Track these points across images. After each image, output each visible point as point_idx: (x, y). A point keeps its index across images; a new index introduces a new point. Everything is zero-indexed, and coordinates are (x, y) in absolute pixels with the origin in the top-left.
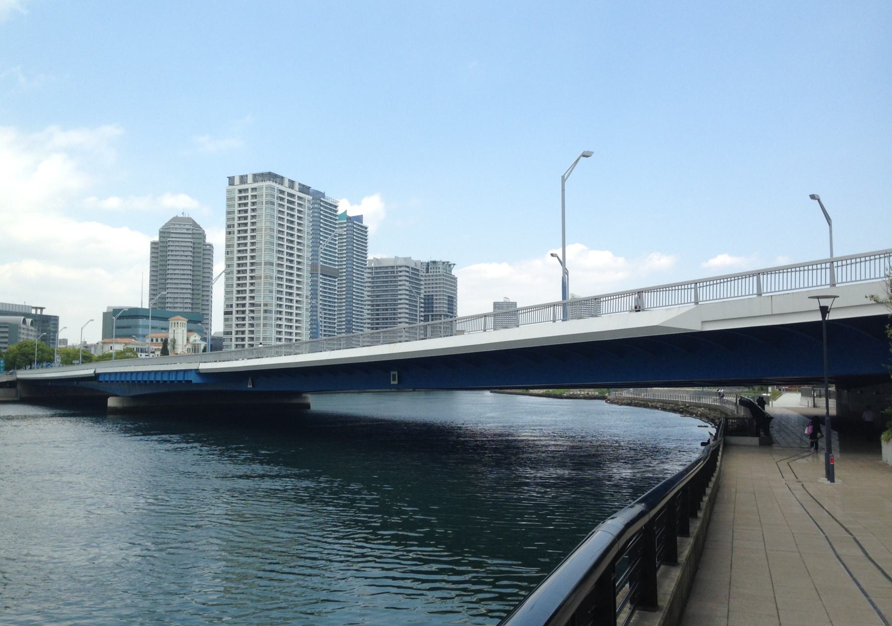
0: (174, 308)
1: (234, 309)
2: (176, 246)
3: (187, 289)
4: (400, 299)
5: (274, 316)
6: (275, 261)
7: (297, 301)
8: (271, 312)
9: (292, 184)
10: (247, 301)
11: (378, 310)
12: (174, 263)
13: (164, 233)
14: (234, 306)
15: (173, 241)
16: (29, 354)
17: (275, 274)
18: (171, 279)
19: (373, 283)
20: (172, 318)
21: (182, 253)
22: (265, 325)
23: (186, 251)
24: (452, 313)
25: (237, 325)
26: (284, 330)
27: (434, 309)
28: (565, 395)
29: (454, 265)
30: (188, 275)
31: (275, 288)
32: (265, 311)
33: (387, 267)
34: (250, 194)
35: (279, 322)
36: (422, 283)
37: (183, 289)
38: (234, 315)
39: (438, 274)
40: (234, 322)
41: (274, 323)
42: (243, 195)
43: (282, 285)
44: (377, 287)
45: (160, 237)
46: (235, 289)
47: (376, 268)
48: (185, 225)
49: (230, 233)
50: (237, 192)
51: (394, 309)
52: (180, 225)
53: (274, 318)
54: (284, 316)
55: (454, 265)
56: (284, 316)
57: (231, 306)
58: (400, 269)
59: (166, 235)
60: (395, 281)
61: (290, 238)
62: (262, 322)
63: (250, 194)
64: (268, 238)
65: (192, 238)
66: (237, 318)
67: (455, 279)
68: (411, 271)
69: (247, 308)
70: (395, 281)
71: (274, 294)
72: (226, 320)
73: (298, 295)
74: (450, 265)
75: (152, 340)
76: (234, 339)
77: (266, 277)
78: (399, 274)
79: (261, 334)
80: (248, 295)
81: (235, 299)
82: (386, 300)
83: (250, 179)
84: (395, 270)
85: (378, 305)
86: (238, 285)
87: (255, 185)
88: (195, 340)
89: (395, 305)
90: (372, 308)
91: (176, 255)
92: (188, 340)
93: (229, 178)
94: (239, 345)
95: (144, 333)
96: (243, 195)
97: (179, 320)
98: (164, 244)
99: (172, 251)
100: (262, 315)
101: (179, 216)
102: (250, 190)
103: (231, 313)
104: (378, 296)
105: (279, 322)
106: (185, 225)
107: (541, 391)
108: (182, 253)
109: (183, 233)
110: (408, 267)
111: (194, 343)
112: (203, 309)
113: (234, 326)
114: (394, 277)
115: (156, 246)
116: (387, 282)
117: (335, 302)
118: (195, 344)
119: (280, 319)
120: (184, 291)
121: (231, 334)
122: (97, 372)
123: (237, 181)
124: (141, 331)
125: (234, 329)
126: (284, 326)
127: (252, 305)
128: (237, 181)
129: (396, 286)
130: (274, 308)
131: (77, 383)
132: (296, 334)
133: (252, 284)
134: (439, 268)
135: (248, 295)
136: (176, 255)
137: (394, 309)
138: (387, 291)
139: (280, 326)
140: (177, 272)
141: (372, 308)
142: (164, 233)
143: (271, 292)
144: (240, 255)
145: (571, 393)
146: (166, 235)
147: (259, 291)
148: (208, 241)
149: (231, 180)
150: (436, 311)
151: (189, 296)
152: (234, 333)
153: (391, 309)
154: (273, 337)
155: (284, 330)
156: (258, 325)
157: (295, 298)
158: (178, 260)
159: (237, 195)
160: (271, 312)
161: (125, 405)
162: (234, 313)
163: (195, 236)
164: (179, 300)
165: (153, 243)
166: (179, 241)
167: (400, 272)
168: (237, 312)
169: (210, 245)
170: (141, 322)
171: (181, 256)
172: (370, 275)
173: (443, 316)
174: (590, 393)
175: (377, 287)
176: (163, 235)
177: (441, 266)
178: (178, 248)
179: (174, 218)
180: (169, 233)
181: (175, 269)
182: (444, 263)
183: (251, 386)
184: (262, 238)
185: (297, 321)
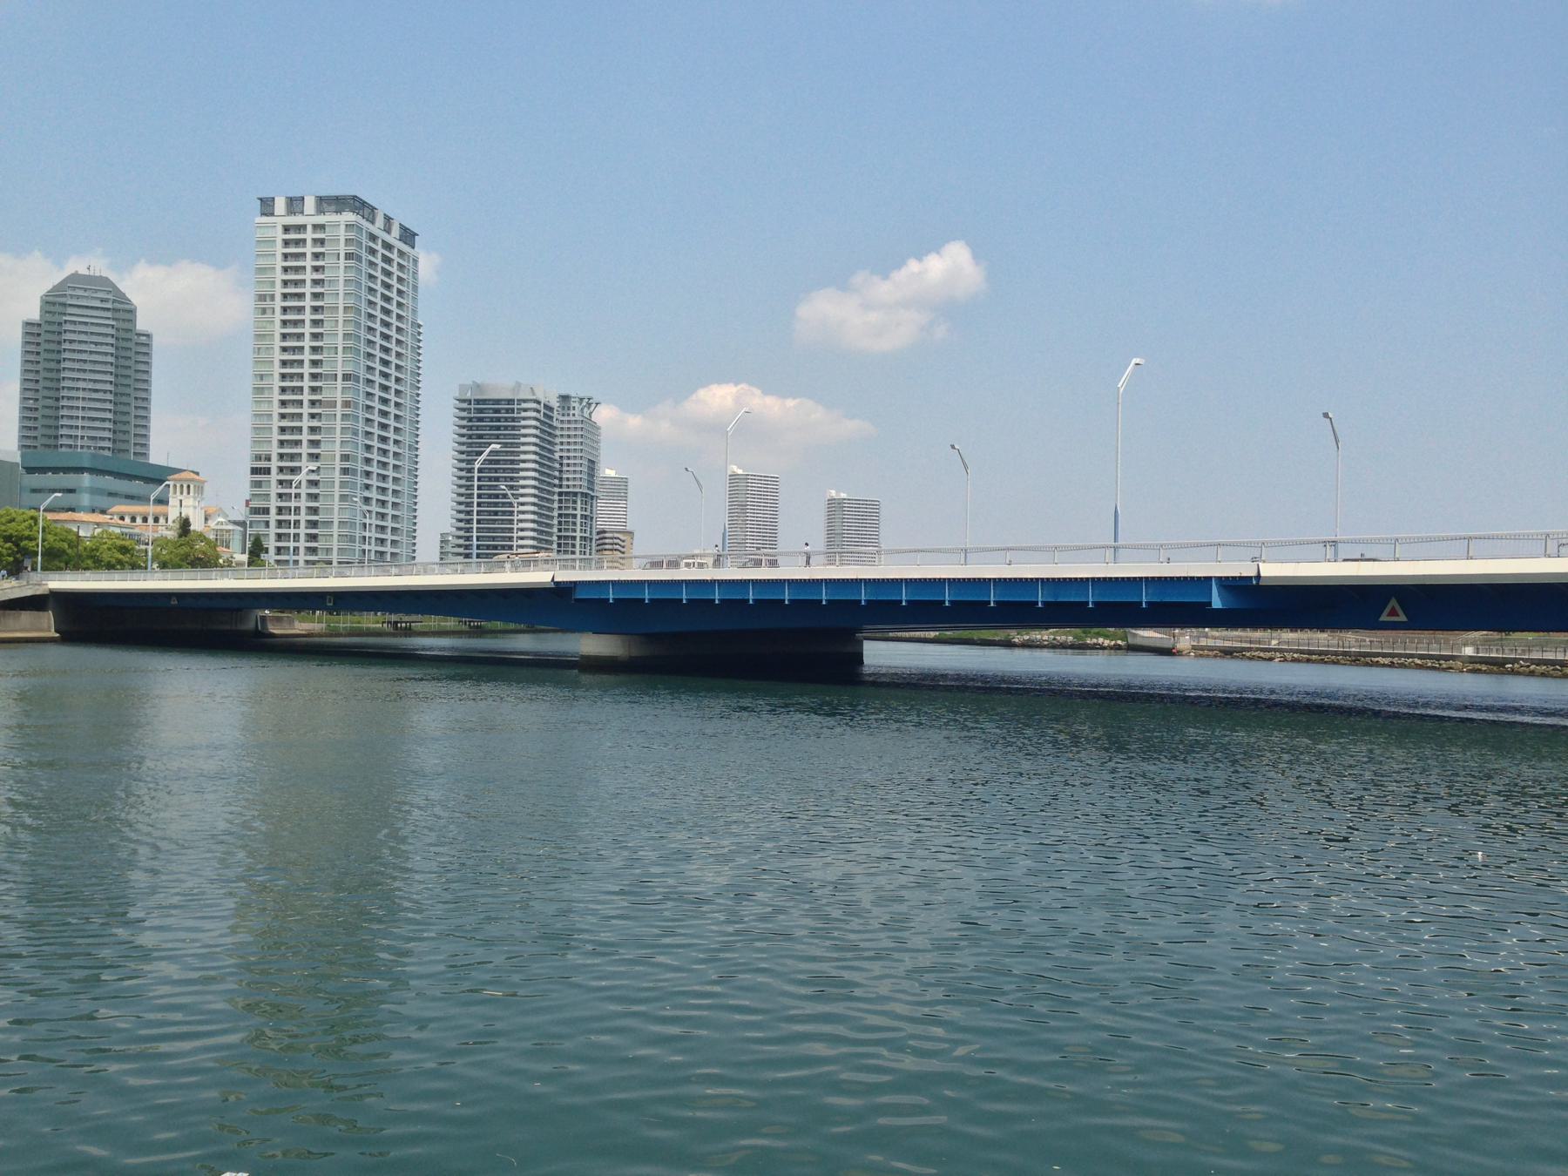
1: (274, 464)
2: (80, 332)
3: (104, 420)
4: (524, 461)
6: (363, 374)
8: (354, 472)
9: (388, 219)
12: (77, 366)
13: (54, 303)
14: (274, 457)
15: (74, 323)
16: (22, 538)
17: (362, 400)
18: (69, 398)
19: (470, 428)
21: (93, 348)
23: (102, 344)
24: (593, 490)
27: (565, 483)
28: (1016, 640)
30: (105, 391)
31: (361, 426)
33: (498, 401)
34: (309, 235)
36: (558, 433)
37: (94, 419)
38: (275, 476)
39: (572, 418)
42: (292, 236)
45: (44, 311)
46: (276, 423)
47: (478, 402)
48: (96, 291)
49: (264, 311)
50: (280, 229)
52: (85, 290)
53: (359, 486)
55: (597, 404)
58: (524, 405)
59: (58, 309)
60: (513, 428)
61: (385, 331)
63: (309, 235)
64: (350, 329)
65: (113, 319)
68: (543, 410)
70: (513, 428)
72: (257, 484)
74: (589, 405)
76: (273, 524)
77: (346, 404)
78: (523, 414)
81: (275, 443)
83: (310, 204)
84: (516, 406)
87: (321, 219)
91: (80, 351)
93: (261, 199)
96: (292, 236)
98: (55, 328)
99: (71, 342)
101: (80, 273)
102: (309, 228)
103: (267, 471)
105: (367, 494)
106: (96, 291)
107: (932, 634)
108: (93, 348)
109: (92, 308)
110: (539, 403)
111: (219, 527)
114: (513, 420)
115: (35, 330)
116: (498, 428)
118: (222, 530)
120: (97, 424)
122: (556, 580)
123: (280, 205)
128: (280, 205)
130: (361, 467)
133: (313, 416)
134: (574, 408)
136: (80, 351)
140: (81, 385)
142: (54, 304)
144: (287, 357)
145: (1026, 637)
146: (58, 309)
147: (331, 430)
148: (141, 325)
149: (267, 206)
150: (568, 486)
152: (273, 511)
153: (505, 477)
157: (392, 448)
158: (85, 361)
159: (280, 236)
160: (354, 472)
161: (635, 652)
162: (274, 471)
163: (117, 315)
165: (28, 324)
166: (86, 323)
167: (525, 410)
168: (281, 469)
169: (148, 336)
171: (91, 352)
173: (579, 496)
174: (1058, 638)
176: (52, 309)
177: (576, 405)
178: (83, 337)
179: (73, 274)
180: (64, 305)
181: (78, 379)
182: (581, 399)
184: (337, 326)
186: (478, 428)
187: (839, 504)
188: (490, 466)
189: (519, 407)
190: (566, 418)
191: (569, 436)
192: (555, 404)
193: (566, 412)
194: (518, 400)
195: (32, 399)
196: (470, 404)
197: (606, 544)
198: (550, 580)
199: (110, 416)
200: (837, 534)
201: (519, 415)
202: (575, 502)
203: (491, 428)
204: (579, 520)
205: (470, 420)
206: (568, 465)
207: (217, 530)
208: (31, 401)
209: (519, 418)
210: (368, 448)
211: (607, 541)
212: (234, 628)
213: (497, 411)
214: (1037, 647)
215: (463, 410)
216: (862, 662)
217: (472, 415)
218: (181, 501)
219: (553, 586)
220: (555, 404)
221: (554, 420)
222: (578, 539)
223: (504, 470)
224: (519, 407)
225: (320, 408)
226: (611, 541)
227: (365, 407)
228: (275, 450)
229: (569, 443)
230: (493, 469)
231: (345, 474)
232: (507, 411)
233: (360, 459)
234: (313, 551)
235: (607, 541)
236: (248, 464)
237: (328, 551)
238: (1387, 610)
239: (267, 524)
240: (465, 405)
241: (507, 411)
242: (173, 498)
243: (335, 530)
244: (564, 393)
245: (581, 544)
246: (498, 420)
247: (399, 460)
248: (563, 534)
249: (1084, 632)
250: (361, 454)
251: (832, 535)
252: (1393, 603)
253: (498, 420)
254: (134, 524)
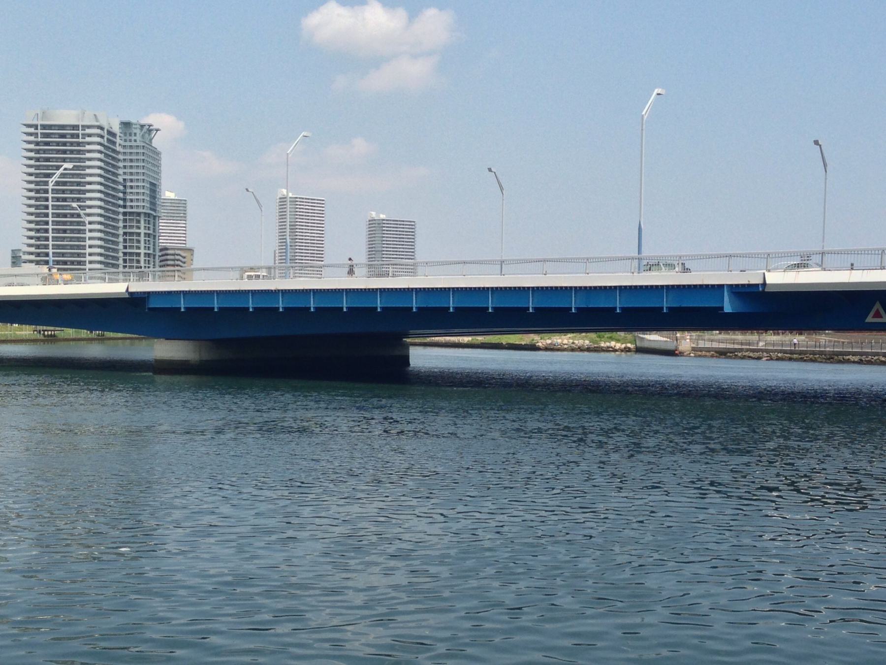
19: (37, 152)
24: (155, 210)
27: (128, 204)
28: (540, 344)
29: (157, 130)
39: (133, 144)
47: (44, 127)
55: (157, 130)
58: (88, 131)
67: (158, 154)
68: (106, 136)
70: (79, 152)
74: (150, 131)
78: (88, 139)
84: (80, 132)
107: (466, 339)
110: (102, 128)
114: (79, 144)
116: (65, 152)
122: (131, 290)
134: (135, 134)
145: (549, 342)
150: (132, 207)
161: (206, 356)
167: (90, 135)
172: (32, 138)
173: (142, 216)
174: (576, 342)
177: (138, 131)
182: (142, 126)
186: (45, 151)
187: (379, 224)
189: (83, 132)
190: (128, 144)
191: (131, 160)
192: (116, 129)
193: (128, 138)
194: (83, 126)
196: (37, 129)
197: (167, 260)
198: (124, 290)
200: (378, 251)
201: (83, 140)
202: (138, 221)
203: (58, 152)
204: (142, 238)
205: (37, 144)
206: (131, 187)
209: (82, 143)
211: (169, 257)
213: (63, 136)
214: (558, 350)
215: (31, 134)
216: (409, 364)
217: (39, 139)
219: (127, 296)
220: (116, 129)
221: (117, 145)
222: (142, 255)
223: (72, 192)
224: (83, 132)
226: (172, 257)
229: (131, 167)
232: (73, 136)
235: (169, 257)
238: (872, 313)
240: (32, 130)
241: (73, 136)
244: (125, 120)
245: (145, 260)
246: (64, 144)
248: (128, 250)
249: (599, 337)
251: (373, 251)
252: (878, 306)
253: (64, 144)
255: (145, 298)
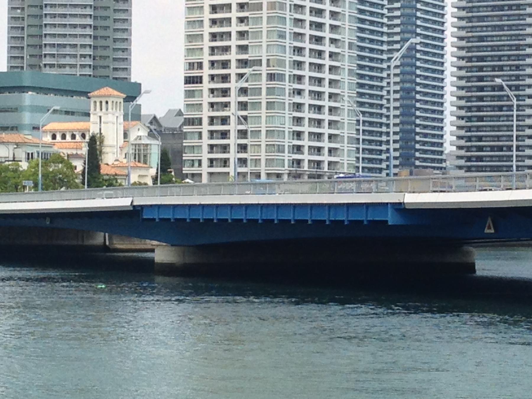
0: (60, 66)
1: (206, 72)
3: (84, 26)
5: (288, 85)
7: (331, 55)
8: (281, 77)
10: (233, 56)
11: (481, 69)
14: (206, 65)
20: (96, 93)
22: (270, 105)
25: (212, 105)
26: (306, 114)
31: (289, 28)
32: (271, 77)
35: (297, 99)
37: (75, 26)
38: (207, 85)
40: (207, 99)
41: (288, 100)
43: (301, 21)
44: (481, 19)
46: (207, 30)
51: (518, 67)
53: (287, 92)
54: (306, 86)
56: (306, 86)
57: (200, 65)
62: (264, 98)
66: (212, 91)
69: (233, 70)
71: (288, 40)
72: (189, 94)
73: (333, 41)
75: (54, 137)
76: (205, 135)
79: (263, 124)
80: (234, 42)
81: (206, 51)
82: (498, 48)
85: (481, 59)
86: (214, 22)
88: (140, 138)
89: (519, 57)
90: (469, 64)
92: (126, 135)
94: (216, 145)
95: (36, 123)
97: (110, 96)
100: (264, 84)
103: (198, 80)
104: (481, 39)
105: (297, 99)
112: (115, 69)
113: (206, 106)
117: (382, 52)
118: (139, 145)
119: (299, 92)
121: (201, 124)
122: (135, 204)
124: (27, 118)
125: (206, 113)
126: (307, 107)
127: (243, 63)
129: (520, 17)
131: (51, 222)
132: (331, 123)
133: (241, 20)
135: (234, 42)
137: (518, 67)
138: (501, 28)
139: (298, 107)
141: (469, 64)
143: (282, 36)
147: (258, 34)
151: (88, 41)
152: (205, 121)
153: (510, 66)
154: (287, 130)
155: (306, 114)
156: (257, 105)
157: (327, 48)
160: (281, 77)
161: (189, 260)
162: (206, 79)
164: (68, 51)
168: (212, 77)
170: (28, 98)
175: (481, 19)
183: (492, 231)
185: (331, 96)
188: (493, 53)
195: (18, 8)
198: (129, 204)
199: (90, 21)
207: (136, 145)
208: (19, 11)
210: (299, 50)
212: (80, 243)
216: (474, 271)
218: (100, 117)
219: (132, 209)
225: (248, 11)
227: (293, 7)
228: (206, 58)
230: (495, 56)
231: (271, 80)
233: (287, 63)
234: (243, 162)
236: (181, 73)
237: (257, 162)
238: (486, 228)
239: (200, 134)
242: (94, 114)
243: (263, 139)
247: (337, 61)
250: (289, 57)
254: (73, 141)
255: (139, 210)
